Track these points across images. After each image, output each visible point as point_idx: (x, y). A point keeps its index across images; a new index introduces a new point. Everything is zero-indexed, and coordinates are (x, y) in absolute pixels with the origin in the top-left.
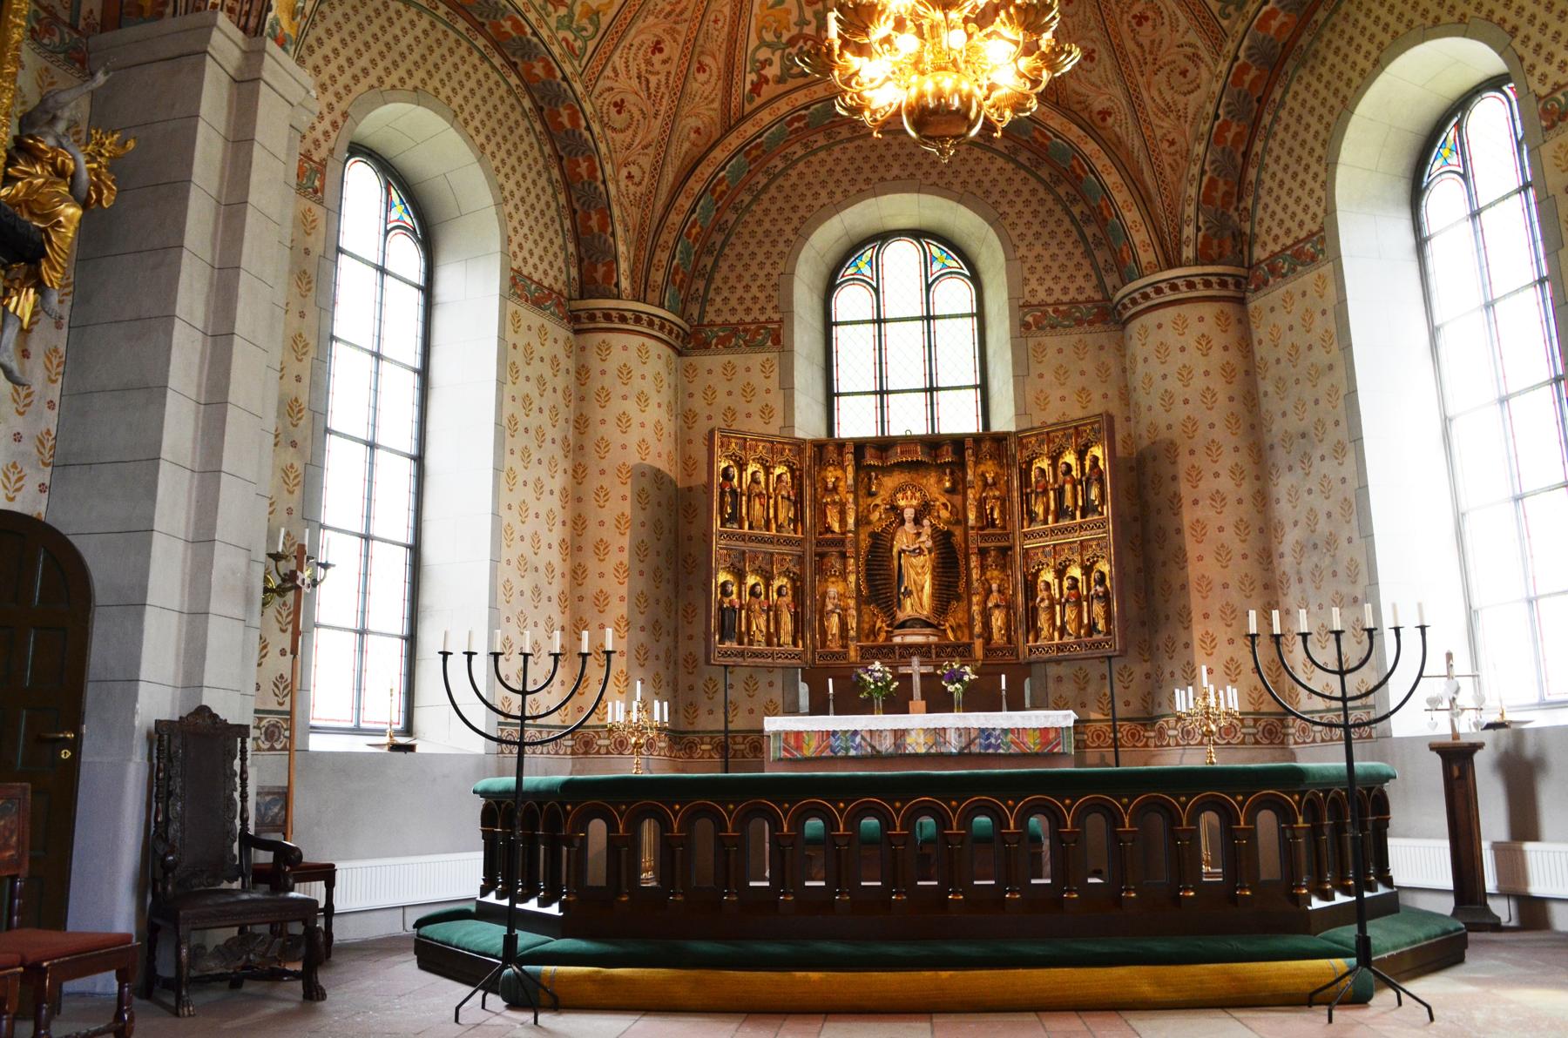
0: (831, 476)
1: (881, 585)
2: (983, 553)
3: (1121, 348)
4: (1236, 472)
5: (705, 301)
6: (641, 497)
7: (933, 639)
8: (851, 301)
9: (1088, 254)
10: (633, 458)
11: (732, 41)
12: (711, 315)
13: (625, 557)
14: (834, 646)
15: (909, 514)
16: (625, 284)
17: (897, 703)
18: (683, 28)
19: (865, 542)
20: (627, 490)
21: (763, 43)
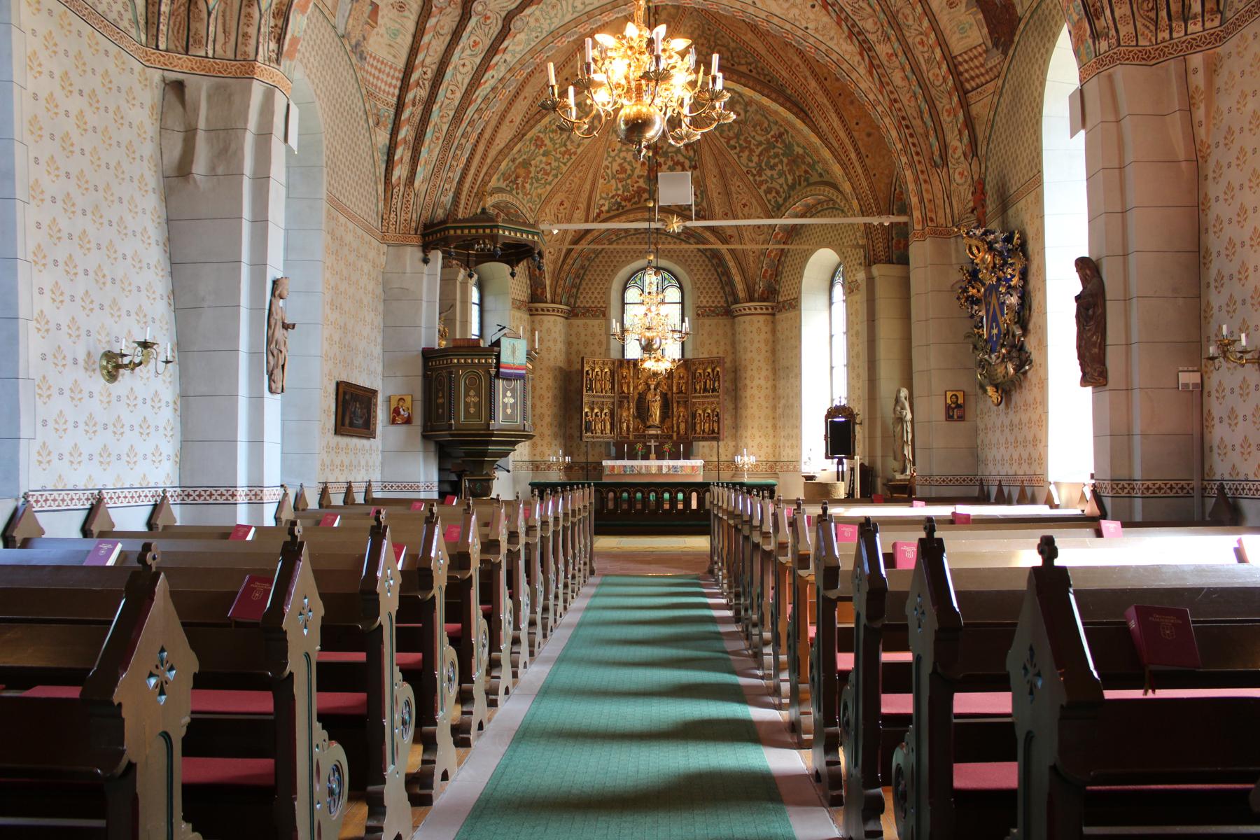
0: (625, 372)
1: (642, 412)
3: (733, 326)
4: (767, 378)
5: (576, 297)
8: (632, 295)
9: (723, 288)
10: (552, 364)
11: (590, 198)
12: (578, 303)
14: (624, 434)
17: (646, 457)
19: (636, 397)
20: (550, 376)
21: (602, 198)
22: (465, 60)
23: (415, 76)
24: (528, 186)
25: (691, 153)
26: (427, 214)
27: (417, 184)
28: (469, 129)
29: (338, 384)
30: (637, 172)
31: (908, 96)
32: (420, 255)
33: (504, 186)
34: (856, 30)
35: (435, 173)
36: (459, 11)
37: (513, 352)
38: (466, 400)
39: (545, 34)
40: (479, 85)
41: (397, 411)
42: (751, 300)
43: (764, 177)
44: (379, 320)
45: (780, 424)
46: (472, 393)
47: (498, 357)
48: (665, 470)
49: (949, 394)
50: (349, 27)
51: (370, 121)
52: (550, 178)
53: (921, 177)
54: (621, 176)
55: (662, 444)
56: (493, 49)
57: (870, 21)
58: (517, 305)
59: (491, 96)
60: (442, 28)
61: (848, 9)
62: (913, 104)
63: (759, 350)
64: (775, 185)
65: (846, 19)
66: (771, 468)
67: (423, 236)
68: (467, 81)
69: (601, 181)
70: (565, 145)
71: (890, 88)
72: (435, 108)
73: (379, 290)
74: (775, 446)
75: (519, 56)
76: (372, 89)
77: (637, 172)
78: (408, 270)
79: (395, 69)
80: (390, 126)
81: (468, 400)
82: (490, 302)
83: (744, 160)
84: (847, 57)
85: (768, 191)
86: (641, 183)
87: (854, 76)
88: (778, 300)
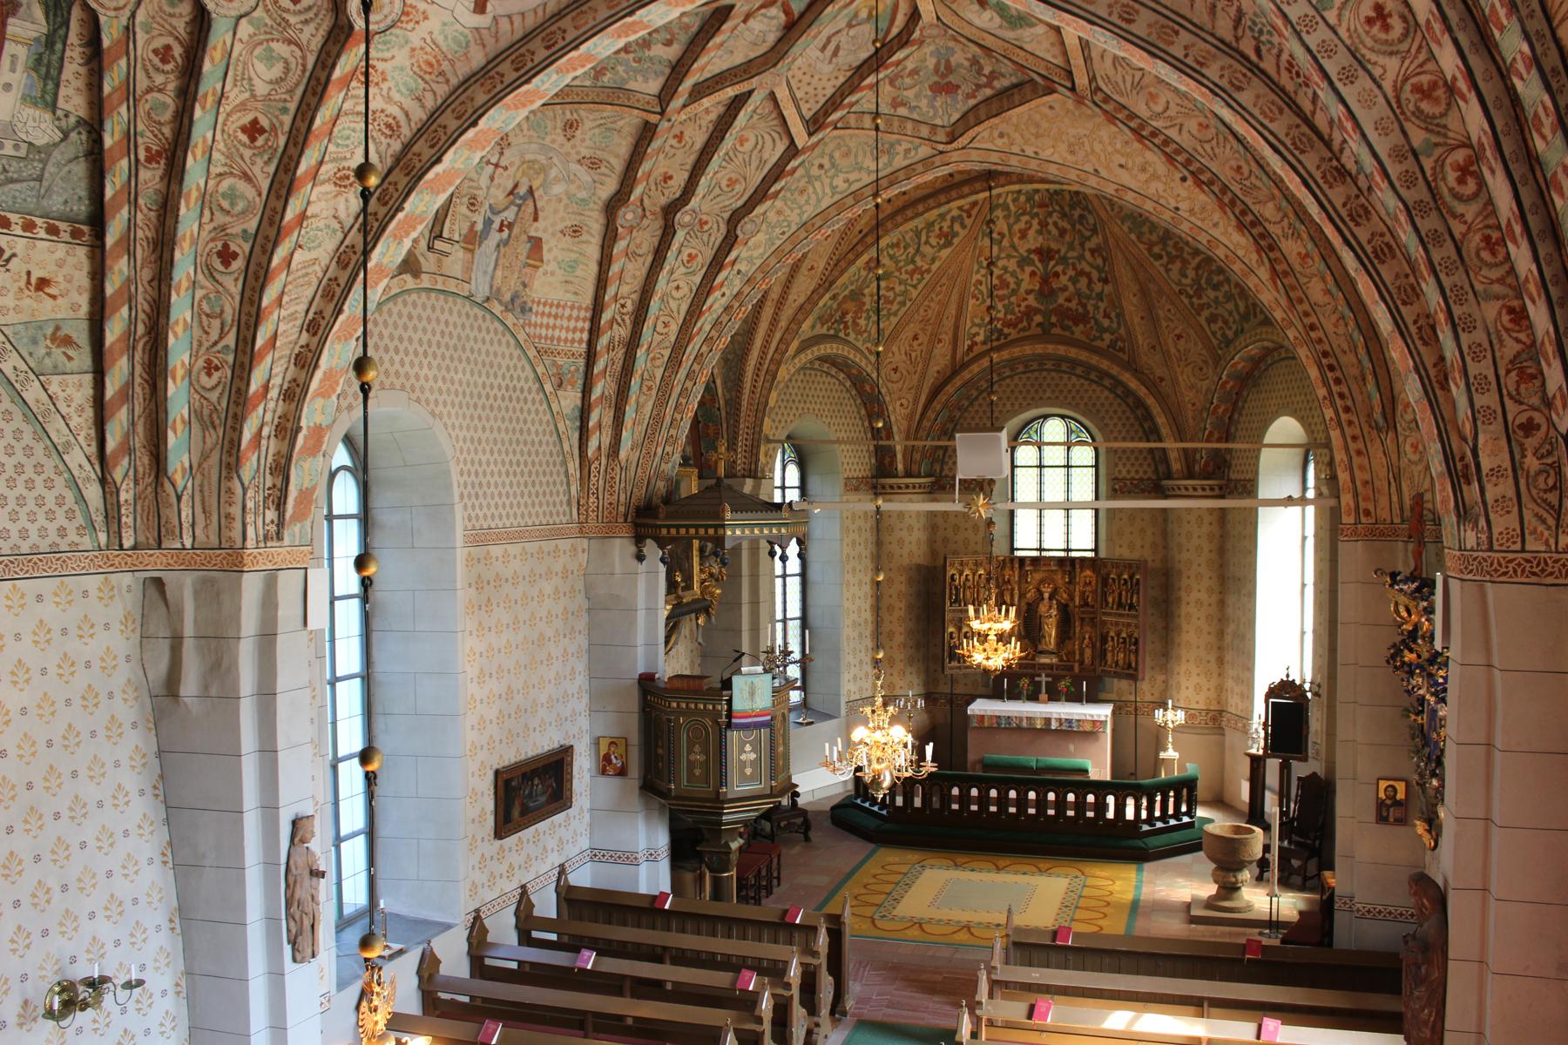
2: (1082, 620)
4: (1210, 590)
6: (910, 581)
7: (1055, 660)
10: (906, 561)
11: (956, 327)
13: (902, 613)
15: (1046, 596)
16: (900, 467)
18: (929, 328)
20: (903, 579)
21: (974, 325)
22: (677, 284)
23: (606, 316)
24: (862, 322)
25: (1099, 261)
26: (640, 493)
27: (623, 455)
28: (696, 367)
29: (497, 773)
30: (1025, 286)
31: (1334, 318)
32: (633, 549)
33: (824, 331)
34: (1250, 218)
35: (649, 435)
36: (659, 223)
37: (752, 694)
38: (689, 756)
39: (794, 228)
40: (701, 313)
41: (607, 758)
42: (1191, 476)
43: (1205, 300)
44: (582, 641)
45: (1228, 658)
46: (697, 748)
47: (730, 702)
48: (1054, 725)
49: (1383, 784)
50: (498, 281)
51: (548, 388)
52: (895, 307)
53: (1352, 446)
54: (1000, 293)
55: (1057, 678)
56: (717, 264)
57: (1270, 205)
58: (853, 486)
59: (725, 319)
60: (639, 246)
61: (1235, 188)
62: (1341, 330)
63: (1199, 548)
64: (1220, 310)
65: (1233, 203)
66: (1214, 719)
67: (636, 525)
68: (684, 307)
69: (972, 302)
70: (913, 262)
71: (1306, 306)
72: (640, 353)
73: (580, 600)
74: (1220, 689)
75: (758, 262)
76: (543, 344)
77: (1025, 286)
78: (618, 569)
79: (580, 308)
80: (580, 382)
81: (692, 757)
82: (814, 484)
83: (1175, 274)
84: (1240, 253)
85: (1212, 319)
86: (1031, 301)
87: (1251, 282)
88: (1231, 479)
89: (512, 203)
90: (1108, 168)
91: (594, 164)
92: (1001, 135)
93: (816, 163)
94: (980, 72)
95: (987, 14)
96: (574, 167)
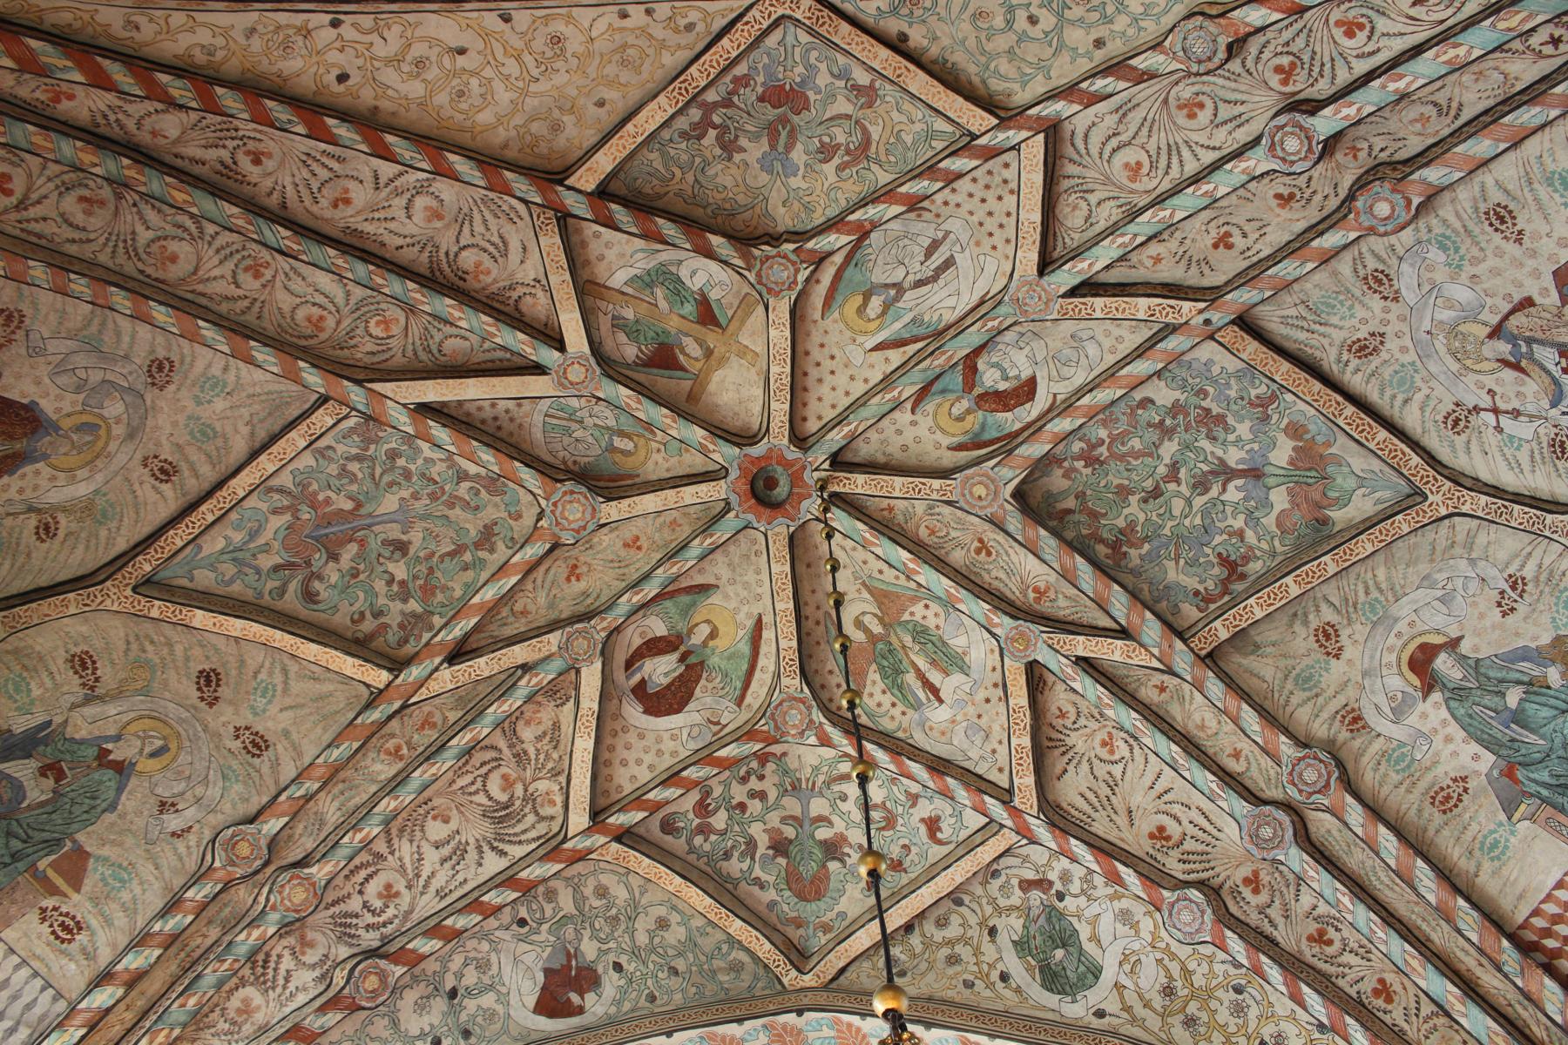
89: (1530, 357)
90: (486, 35)
91: (1379, 282)
92: (690, 27)
93: (1036, 32)
94: (723, 129)
95: (696, 283)
96: (1409, 296)
